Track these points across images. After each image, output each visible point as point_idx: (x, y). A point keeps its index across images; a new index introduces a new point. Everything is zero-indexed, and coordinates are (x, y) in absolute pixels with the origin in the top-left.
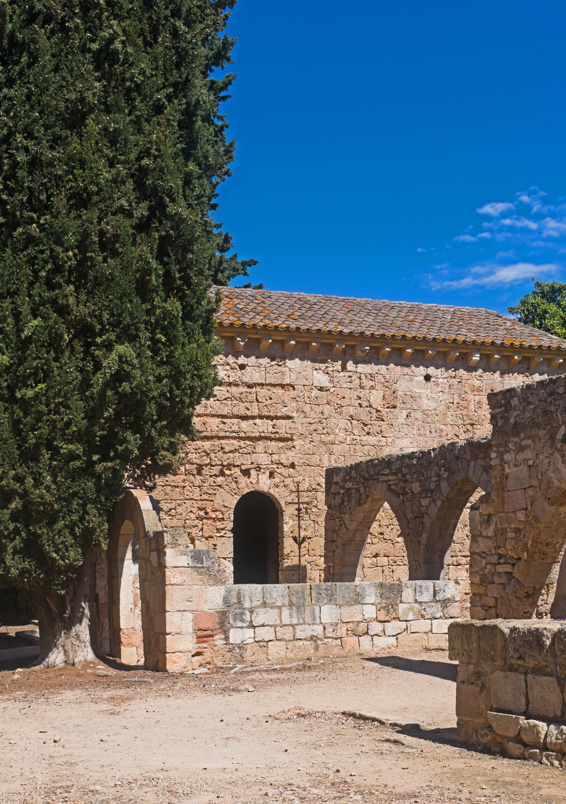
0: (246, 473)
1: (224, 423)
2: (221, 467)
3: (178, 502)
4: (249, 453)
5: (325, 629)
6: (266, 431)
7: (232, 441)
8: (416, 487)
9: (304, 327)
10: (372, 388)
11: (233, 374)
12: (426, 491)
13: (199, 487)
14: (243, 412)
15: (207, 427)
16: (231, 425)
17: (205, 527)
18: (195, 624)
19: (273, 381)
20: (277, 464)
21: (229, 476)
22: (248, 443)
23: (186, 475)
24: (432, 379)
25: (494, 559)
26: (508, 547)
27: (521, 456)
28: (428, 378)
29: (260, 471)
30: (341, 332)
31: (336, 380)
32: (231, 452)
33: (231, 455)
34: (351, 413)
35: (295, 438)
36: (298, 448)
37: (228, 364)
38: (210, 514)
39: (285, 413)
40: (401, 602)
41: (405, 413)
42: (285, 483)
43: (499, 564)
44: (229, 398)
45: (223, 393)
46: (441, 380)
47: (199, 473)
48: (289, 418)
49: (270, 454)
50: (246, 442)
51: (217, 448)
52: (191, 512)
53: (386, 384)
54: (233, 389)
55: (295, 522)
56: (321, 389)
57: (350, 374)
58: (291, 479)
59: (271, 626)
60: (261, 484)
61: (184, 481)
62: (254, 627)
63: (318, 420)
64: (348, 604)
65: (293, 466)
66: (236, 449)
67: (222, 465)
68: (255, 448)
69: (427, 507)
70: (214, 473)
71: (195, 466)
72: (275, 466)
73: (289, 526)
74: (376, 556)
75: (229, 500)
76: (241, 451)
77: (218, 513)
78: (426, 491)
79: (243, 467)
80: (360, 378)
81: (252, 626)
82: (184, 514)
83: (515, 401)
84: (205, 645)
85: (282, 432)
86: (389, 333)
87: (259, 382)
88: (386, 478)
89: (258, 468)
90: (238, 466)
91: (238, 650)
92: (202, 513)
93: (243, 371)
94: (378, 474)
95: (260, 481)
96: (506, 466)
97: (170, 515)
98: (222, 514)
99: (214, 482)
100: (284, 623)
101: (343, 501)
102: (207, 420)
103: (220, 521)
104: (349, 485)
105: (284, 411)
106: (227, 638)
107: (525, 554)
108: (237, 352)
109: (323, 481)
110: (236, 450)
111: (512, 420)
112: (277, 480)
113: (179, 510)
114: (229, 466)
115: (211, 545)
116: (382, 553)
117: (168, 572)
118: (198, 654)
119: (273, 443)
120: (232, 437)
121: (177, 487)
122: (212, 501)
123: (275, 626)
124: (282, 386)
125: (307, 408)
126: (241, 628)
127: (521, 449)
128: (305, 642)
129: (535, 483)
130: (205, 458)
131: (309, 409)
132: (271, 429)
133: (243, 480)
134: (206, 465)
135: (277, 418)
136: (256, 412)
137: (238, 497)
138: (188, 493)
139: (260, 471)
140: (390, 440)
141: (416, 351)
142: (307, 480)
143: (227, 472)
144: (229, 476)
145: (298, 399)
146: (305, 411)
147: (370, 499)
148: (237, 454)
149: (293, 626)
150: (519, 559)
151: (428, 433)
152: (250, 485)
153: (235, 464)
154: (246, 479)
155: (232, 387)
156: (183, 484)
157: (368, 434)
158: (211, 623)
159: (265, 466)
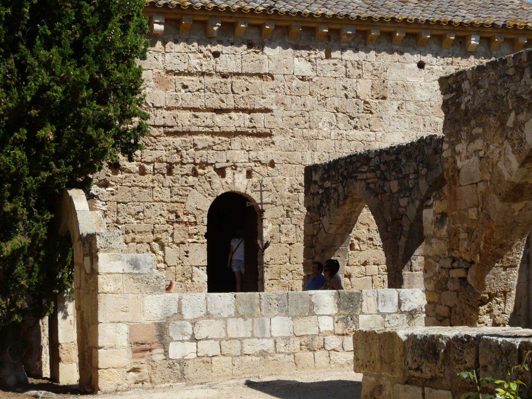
0: (221, 172)
1: (197, 117)
2: (193, 165)
3: (146, 204)
4: (224, 150)
5: (275, 343)
6: (242, 125)
7: (205, 137)
8: (394, 186)
9: (283, 10)
10: (360, 76)
11: (206, 63)
12: (404, 190)
13: (170, 187)
14: (217, 105)
15: (178, 121)
16: (204, 119)
17: (176, 232)
18: (130, 337)
19: (250, 70)
20: (255, 161)
21: (202, 175)
22: (223, 138)
23: (154, 174)
24: (426, 67)
25: (447, 263)
26: (462, 249)
27: (473, 147)
28: (421, 65)
29: (236, 169)
30: (323, 15)
31: (319, 68)
32: (204, 148)
33: (204, 152)
34: (337, 105)
35: (274, 133)
36: (277, 144)
37: (201, 52)
38: (181, 217)
39: (264, 105)
40: (362, 313)
41: (396, 104)
43: (453, 268)
44: (201, 89)
45: (195, 84)
46: (436, 67)
47: (170, 172)
48: (267, 110)
49: (248, 151)
50: (221, 138)
51: (189, 145)
52: (161, 215)
53: (375, 72)
54: (207, 80)
55: (275, 227)
56: (303, 79)
57: (335, 61)
58: (270, 179)
59: (216, 340)
60: (237, 184)
61: (153, 181)
62: (197, 341)
63: (300, 112)
64: (302, 316)
65: (272, 164)
66: (209, 146)
67: (195, 164)
68: (230, 145)
69: (405, 207)
70: (185, 172)
72: (252, 164)
74: (365, 264)
75: (202, 203)
76: (215, 148)
77: (190, 217)
78: (404, 190)
79: (218, 166)
80: (346, 67)
81: (194, 339)
82: (153, 217)
83: (466, 86)
84: (143, 361)
85: (260, 127)
86: (376, 15)
87: (235, 71)
88: (365, 176)
89: (234, 167)
90: (211, 164)
91: (178, 367)
93: (217, 59)
94: (356, 171)
96: (458, 159)
97: (137, 219)
98: (195, 217)
99: (186, 182)
100: (231, 335)
101: (322, 202)
102: (178, 114)
103: (192, 225)
104: (328, 184)
105: (261, 103)
106: (166, 353)
107: (478, 258)
108: (211, 38)
109: (302, 179)
110: (210, 147)
111: (463, 107)
112: (255, 179)
113: (148, 213)
114: (204, 165)
115: (182, 252)
116: (371, 260)
117: (100, 279)
118: (135, 370)
119: (250, 139)
121: (145, 187)
122: (183, 203)
123: (220, 340)
124: (260, 76)
126: (182, 341)
127: (472, 139)
128: (254, 358)
129: (487, 177)
131: (290, 101)
132: (248, 123)
133: (217, 180)
134: (177, 163)
135: (254, 111)
136: (230, 104)
137: (212, 199)
139: (236, 169)
140: (379, 134)
141: (409, 35)
142: (287, 179)
143: (200, 171)
144: (202, 175)
145: (277, 90)
146: (285, 103)
147: (349, 199)
148: (210, 151)
149: (241, 340)
150: (473, 263)
151: (421, 126)
153: (209, 162)
155: (205, 76)
157: (355, 128)
158: (150, 336)
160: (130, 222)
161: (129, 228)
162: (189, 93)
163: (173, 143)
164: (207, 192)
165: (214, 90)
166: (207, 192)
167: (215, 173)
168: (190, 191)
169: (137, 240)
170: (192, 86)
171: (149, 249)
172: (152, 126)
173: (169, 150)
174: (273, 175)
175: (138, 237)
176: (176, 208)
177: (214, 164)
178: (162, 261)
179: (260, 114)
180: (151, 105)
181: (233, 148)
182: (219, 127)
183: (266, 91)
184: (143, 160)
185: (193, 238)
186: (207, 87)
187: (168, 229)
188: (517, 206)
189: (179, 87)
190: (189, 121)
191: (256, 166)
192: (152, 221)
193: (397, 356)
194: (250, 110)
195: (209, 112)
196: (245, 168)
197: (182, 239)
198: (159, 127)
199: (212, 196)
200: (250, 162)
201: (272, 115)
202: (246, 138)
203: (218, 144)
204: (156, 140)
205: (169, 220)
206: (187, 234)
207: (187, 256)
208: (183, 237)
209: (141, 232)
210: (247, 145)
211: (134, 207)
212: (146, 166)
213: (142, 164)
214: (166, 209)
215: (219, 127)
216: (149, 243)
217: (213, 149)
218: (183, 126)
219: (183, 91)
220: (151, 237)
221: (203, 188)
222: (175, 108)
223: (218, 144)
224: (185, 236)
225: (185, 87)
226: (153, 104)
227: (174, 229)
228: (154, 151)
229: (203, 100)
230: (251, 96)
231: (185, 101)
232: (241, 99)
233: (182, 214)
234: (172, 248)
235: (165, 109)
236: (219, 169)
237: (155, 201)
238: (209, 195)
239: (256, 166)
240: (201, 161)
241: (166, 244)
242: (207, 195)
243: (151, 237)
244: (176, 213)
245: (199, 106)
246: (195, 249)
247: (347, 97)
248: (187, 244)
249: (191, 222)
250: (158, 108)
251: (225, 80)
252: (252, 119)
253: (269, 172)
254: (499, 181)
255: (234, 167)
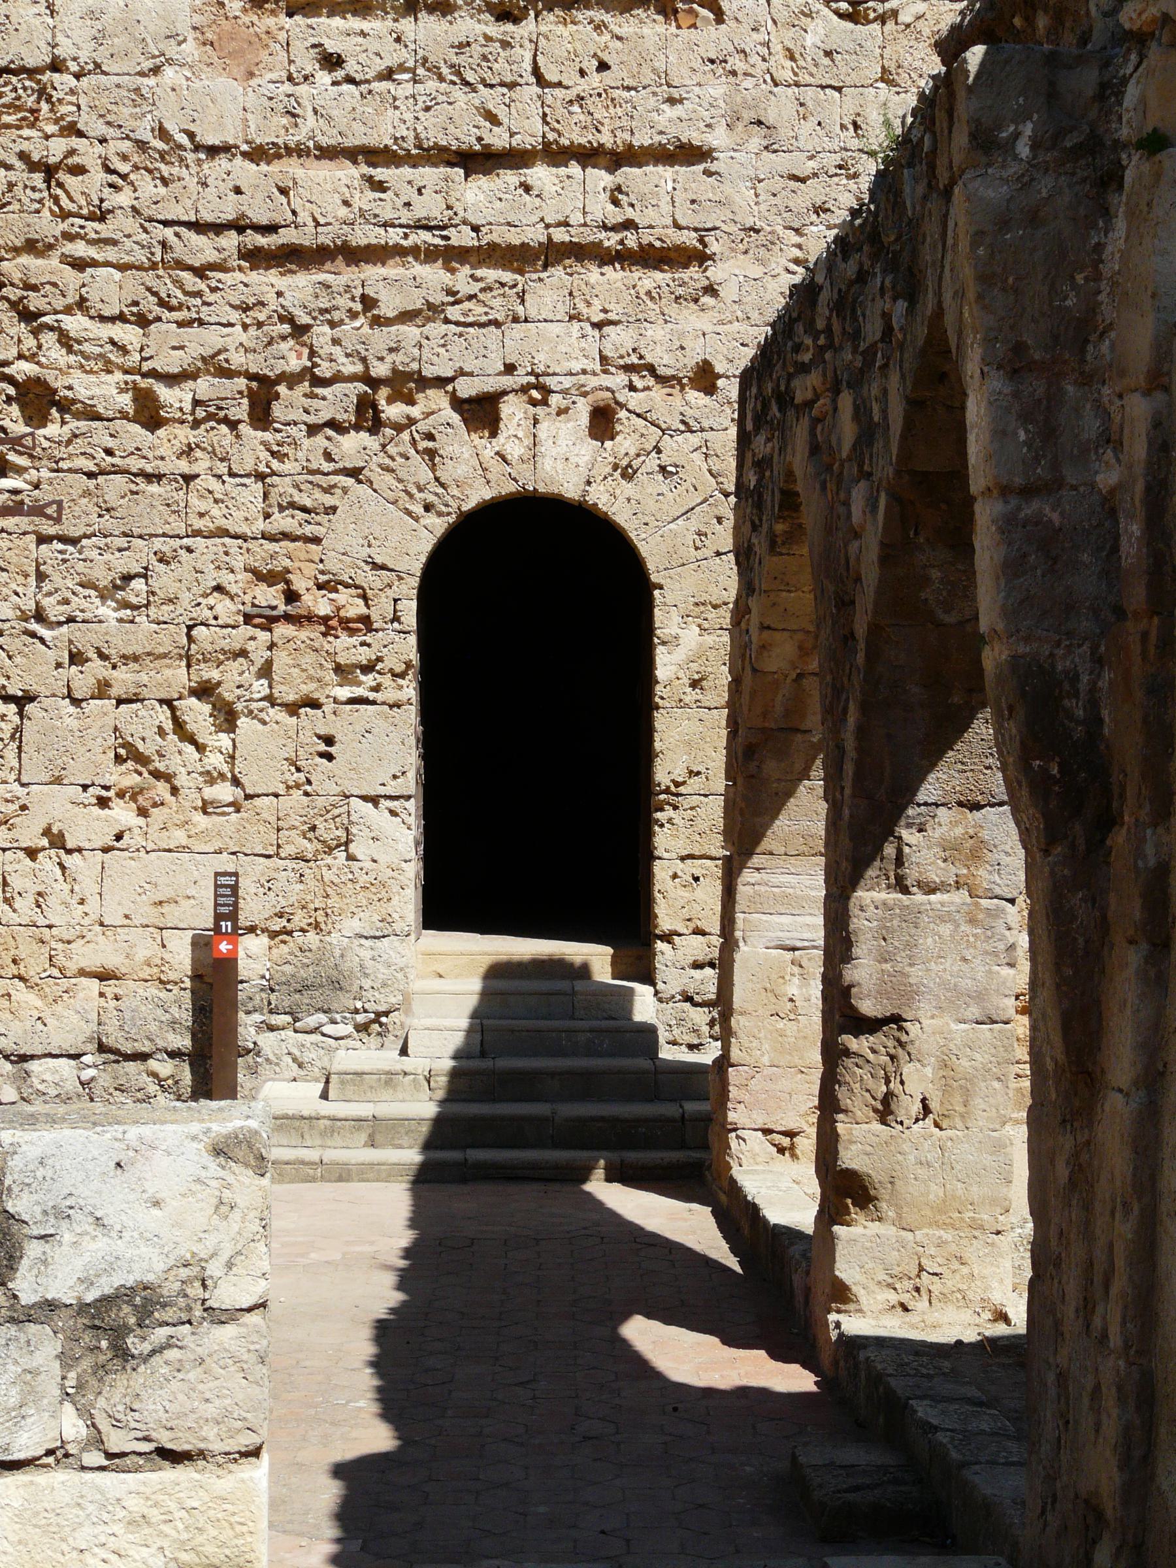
1: (379, 186)
2: (362, 388)
4: (496, 324)
6: (576, 218)
13: (260, 477)
16: (410, 194)
17: (281, 660)
20: (629, 368)
21: (399, 428)
22: (491, 274)
29: (545, 402)
32: (406, 317)
33: (410, 332)
35: (714, 247)
36: (728, 292)
39: (673, 132)
42: (665, 459)
44: (402, 68)
45: (373, 45)
47: (261, 416)
49: (598, 326)
50: (479, 273)
51: (344, 302)
52: (219, 588)
55: (709, 639)
58: (695, 440)
60: (547, 465)
61: (188, 451)
66: (430, 306)
70: (325, 416)
71: (241, 383)
72: (619, 380)
73: (680, 654)
75: (394, 539)
76: (454, 313)
77: (343, 596)
79: (466, 388)
82: (186, 598)
90: (441, 382)
92: (269, 596)
95: (545, 447)
98: (365, 597)
99: (328, 457)
102: (300, 173)
103: (352, 632)
110: (433, 311)
112: (625, 444)
113: (165, 579)
119: (614, 275)
120: (414, 251)
121: (158, 477)
122: (316, 540)
130: (284, 346)
137: (438, 525)
138: (203, 506)
139: (545, 402)
143: (394, 411)
144: (399, 428)
148: (436, 329)
152: (496, 466)
153: (428, 372)
154: (479, 440)
155: (423, 15)
156: (183, 466)
159: (567, 382)
160: (88, 615)
161: (85, 639)
162: (346, 88)
163: (279, 294)
164: (418, 495)
165: (458, 74)
166: (418, 495)
167: (456, 418)
168: (345, 490)
169: (114, 691)
170: (362, 58)
171: (168, 726)
172: (189, 225)
173: (260, 325)
174: (706, 425)
175: (123, 679)
176: (287, 563)
177: (452, 380)
178: (222, 776)
179: (660, 168)
180: (183, 140)
181: (533, 313)
182: (476, 229)
183: (686, 72)
184: (146, 367)
185: (359, 684)
186: (425, 60)
187: (251, 646)
189: (307, 62)
190: (346, 203)
191: (632, 388)
192: (184, 611)
194: (613, 152)
195: (435, 165)
196: (584, 395)
197: (308, 688)
198: (218, 228)
199: (440, 514)
200: (605, 372)
201: (708, 173)
202: (593, 273)
203: (471, 297)
204: (202, 286)
205: (255, 611)
206: (330, 666)
207: (329, 757)
208: (311, 678)
209: (136, 658)
210: (595, 301)
211: (107, 556)
212: (164, 393)
213: (144, 383)
214: (238, 564)
215: (476, 229)
216: (168, 703)
217: (447, 321)
218: (318, 224)
219: (324, 78)
220: (178, 677)
221: (400, 481)
222: (289, 151)
223: (471, 297)
224: (320, 673)
225: (331, 61)
226: (191, 135)
227: (272, 646)
228: (195, 330)
229: (409, 116)
230: (616, 93)
231: (329, 119)
232: (576, 108)
233: (311, 584)
234: (264, 723)
235: (245, 155)
236: (469, 401)
237: (197, 533)
238: (428, 508)
239: (632, 388)
240: (395, 371)
241: (239, 706)
242: (418, 509)
243: (178, 677)
244: (288, 582)
245: (390, 142)
246: (359, 728)
248: (328, 708)
249: (349, 620)
250: (213, 151)
251: (510, 27)
252: (619, 189)
253: (689, 412)
255: (535, 394)
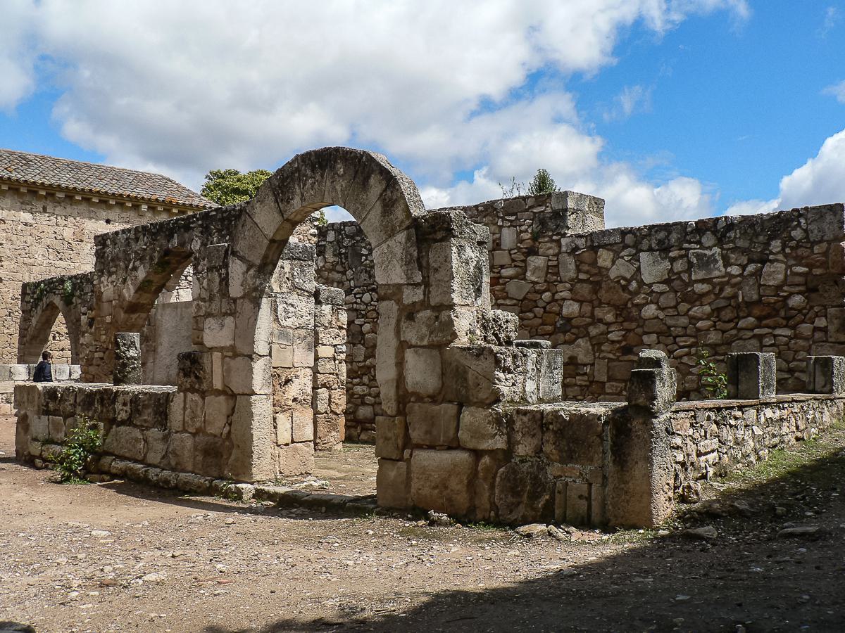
10: (65, 226)
53: (76, 224)
56: (26, 224)
74: (63, 350)
101: (32, 308)
125: (14, 238)
127: (110, 274)
145: (7, 230)
157: (61, 259)
188: (134, 316)
193: (36, 399)
247: (56, 239)
254: (124, 300)
